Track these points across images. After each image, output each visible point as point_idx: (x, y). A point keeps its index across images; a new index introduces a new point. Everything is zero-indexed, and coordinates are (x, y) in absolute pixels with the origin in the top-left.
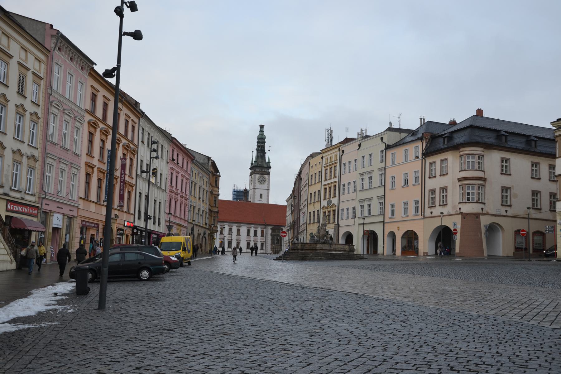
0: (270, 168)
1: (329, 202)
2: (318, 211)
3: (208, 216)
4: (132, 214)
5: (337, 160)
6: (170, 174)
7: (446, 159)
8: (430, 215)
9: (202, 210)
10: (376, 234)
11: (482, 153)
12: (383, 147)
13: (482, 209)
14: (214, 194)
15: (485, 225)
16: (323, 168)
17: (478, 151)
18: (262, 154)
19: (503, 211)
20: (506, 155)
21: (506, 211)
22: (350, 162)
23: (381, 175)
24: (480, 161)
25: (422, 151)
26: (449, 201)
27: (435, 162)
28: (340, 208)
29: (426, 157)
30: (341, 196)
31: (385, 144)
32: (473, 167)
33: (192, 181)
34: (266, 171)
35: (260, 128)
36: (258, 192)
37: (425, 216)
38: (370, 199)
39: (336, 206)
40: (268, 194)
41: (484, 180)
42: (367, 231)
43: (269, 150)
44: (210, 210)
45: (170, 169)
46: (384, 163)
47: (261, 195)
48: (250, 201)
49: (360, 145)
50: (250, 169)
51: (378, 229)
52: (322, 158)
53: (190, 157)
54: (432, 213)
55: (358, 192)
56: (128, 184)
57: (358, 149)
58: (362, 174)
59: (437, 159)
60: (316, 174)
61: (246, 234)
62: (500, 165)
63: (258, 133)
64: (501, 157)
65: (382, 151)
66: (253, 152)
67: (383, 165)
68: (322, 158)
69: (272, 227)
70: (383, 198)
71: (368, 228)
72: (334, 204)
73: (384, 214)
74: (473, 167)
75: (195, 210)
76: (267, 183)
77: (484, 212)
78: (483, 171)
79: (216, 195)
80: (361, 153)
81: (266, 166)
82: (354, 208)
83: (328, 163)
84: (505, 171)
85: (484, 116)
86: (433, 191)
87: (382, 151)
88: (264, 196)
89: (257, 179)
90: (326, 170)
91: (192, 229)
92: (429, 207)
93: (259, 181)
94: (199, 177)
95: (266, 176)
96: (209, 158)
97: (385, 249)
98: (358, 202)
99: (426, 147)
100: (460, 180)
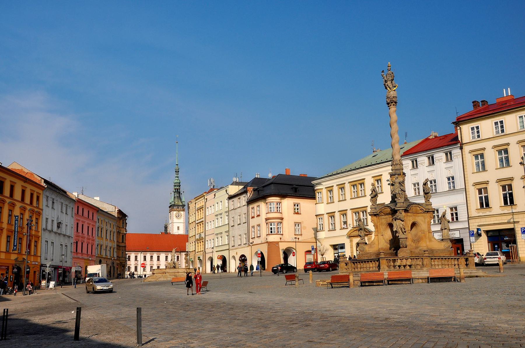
3: (115, 250)
4: (39, 256)
9: (110, 246)
11: (280, 201)
12: (227, 196)
13: (281, 238)
14: (122, 233)
18: (178, 195)
25: (247, 199)
32: (274, 210)
38: (221, 233)
41: (282, 219)
43: (183, 192)
44: (117, 245)
47: (178, 227)
49: (215, 195)
53: (95, 210)
56: (34, 236)
59: (255, 205)
64: (294, 203)
68: (195, 204)
72: (202, 237)
74: (274, 210)
77: (282, 240)
89: (174, 215)
100: (266, 219)
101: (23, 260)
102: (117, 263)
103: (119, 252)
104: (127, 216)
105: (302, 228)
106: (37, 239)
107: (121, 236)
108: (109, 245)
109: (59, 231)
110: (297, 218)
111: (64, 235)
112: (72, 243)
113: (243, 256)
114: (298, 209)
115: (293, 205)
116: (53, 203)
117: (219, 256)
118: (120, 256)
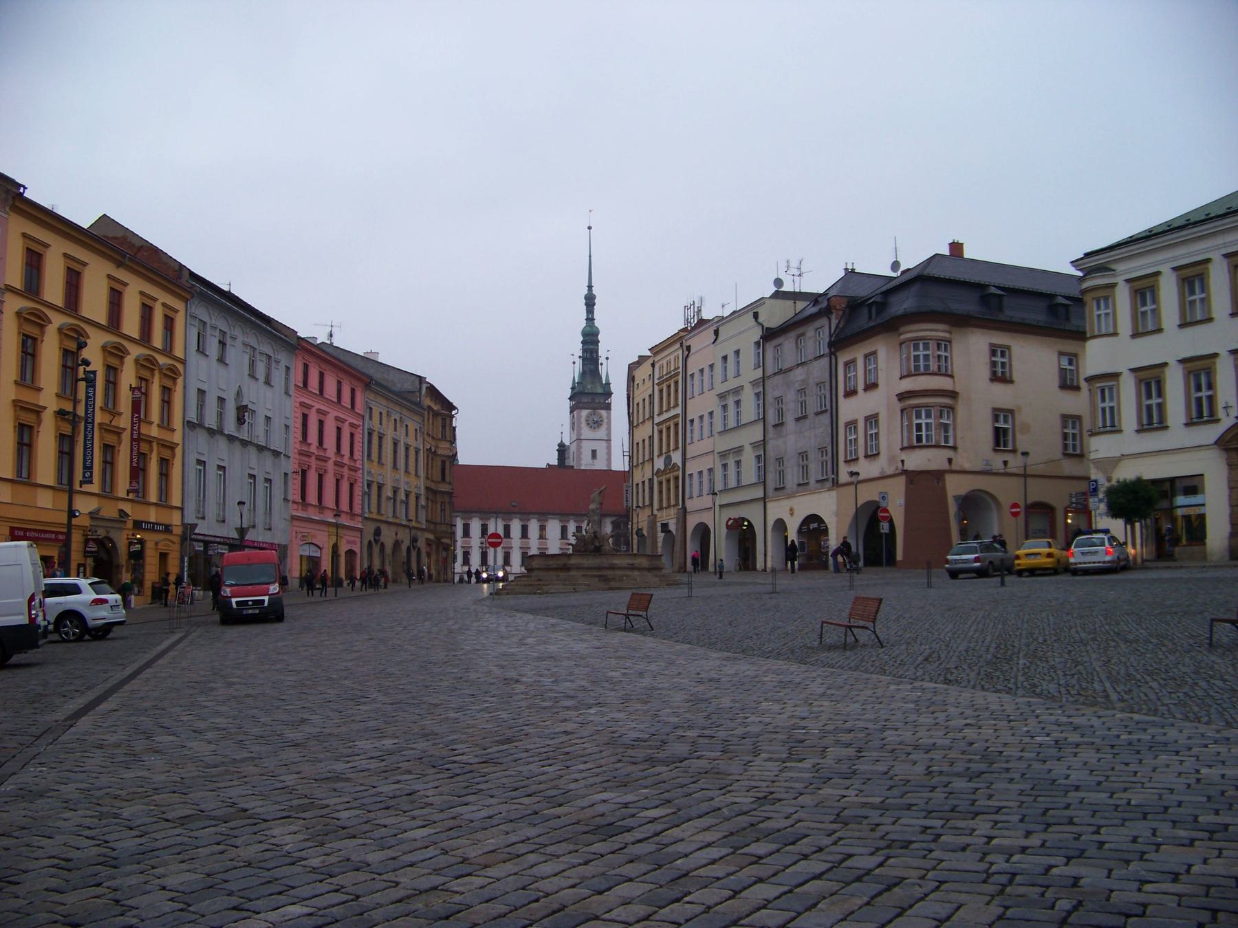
0: (609, 394)
1: (668, 459)
2: (650, 479)
3: (423, 502)
4: (176, 508)
5: (678, 368)
6: (300, 416)
7: (874, 353)
12: (757, 334)
13: (950, 461)
15: (954, 497)
16: (655, 386)
17: (937, 331)
18: (592, 367)
19: (997, 462)
20: (1000, 339)
21: (1005, 463)
22: (702, 371)
24: (942, 353)
25: (831, 336)
27: (854, 361)
28: (688, 472)
29: (837, 350)
30: (688, 448)
31: (763, 326)
33: (369, 429)
34: (602, 401)
35: (587, 312)
36: (587, 448)
38: (739, 450)
39: (679, 467)
40: (609, 448)
41: (953, 395)
43: (607, 358)
44: (427, 488)
45: (298, 405)
47: (594, 453)
48: (572, 467)
49: (716, 333)
50: (571, 399)
51: (753, 515)
52: (653, 365)
53: (359, 379)
55: (716, 436)
56: (158, 444)
57: (714, 343)
58: (722, 396)
59: (858, 353)
60: (644, 400)
61: (559, 535)
62: (988, 361)
63: (584, 324)
64: (991, 345)
65: (757, 343)
66: (574, 363)
67: (759, 373)
68: (653, 365)
69: (614, 519)
71: (735, 513)
75: (384, 490)
76: (604, 426)
77: (954, 467)
78: (951, 376)
79: (443, 456)
80: (720, 350)
81: (600, 391)
82: (710, 470)
83: (663, 377)
84: (1000, 376)
85: (965, 256)
86: (851, 425)
87: (757, 343)
88: (601, 454)
89: (583, 420)
90: (661, 391)
91: (378, 532)
93: (588, 424)
94: (393, 418)
95: (603, 413)
96: (421, 379)
97: (769, 559)
98: (716, 456)
99: (837, 327)
100: (902, 397)
101: (121, 516)
102: (427, 539)
103: (432, 509)
104: (455, 408)
105: (1017, 429)
106: (169, 452)
107: (439, 463)
108: (402, 487)
109: (244, 436)
110: (1002, 395)
111: (261, 449)
112: (286, 474)
113: (813, 518)
114: (1003, 364)
115: (985, 350)
116: (222, 343)
117: (730, 519)
118: (434, 521)
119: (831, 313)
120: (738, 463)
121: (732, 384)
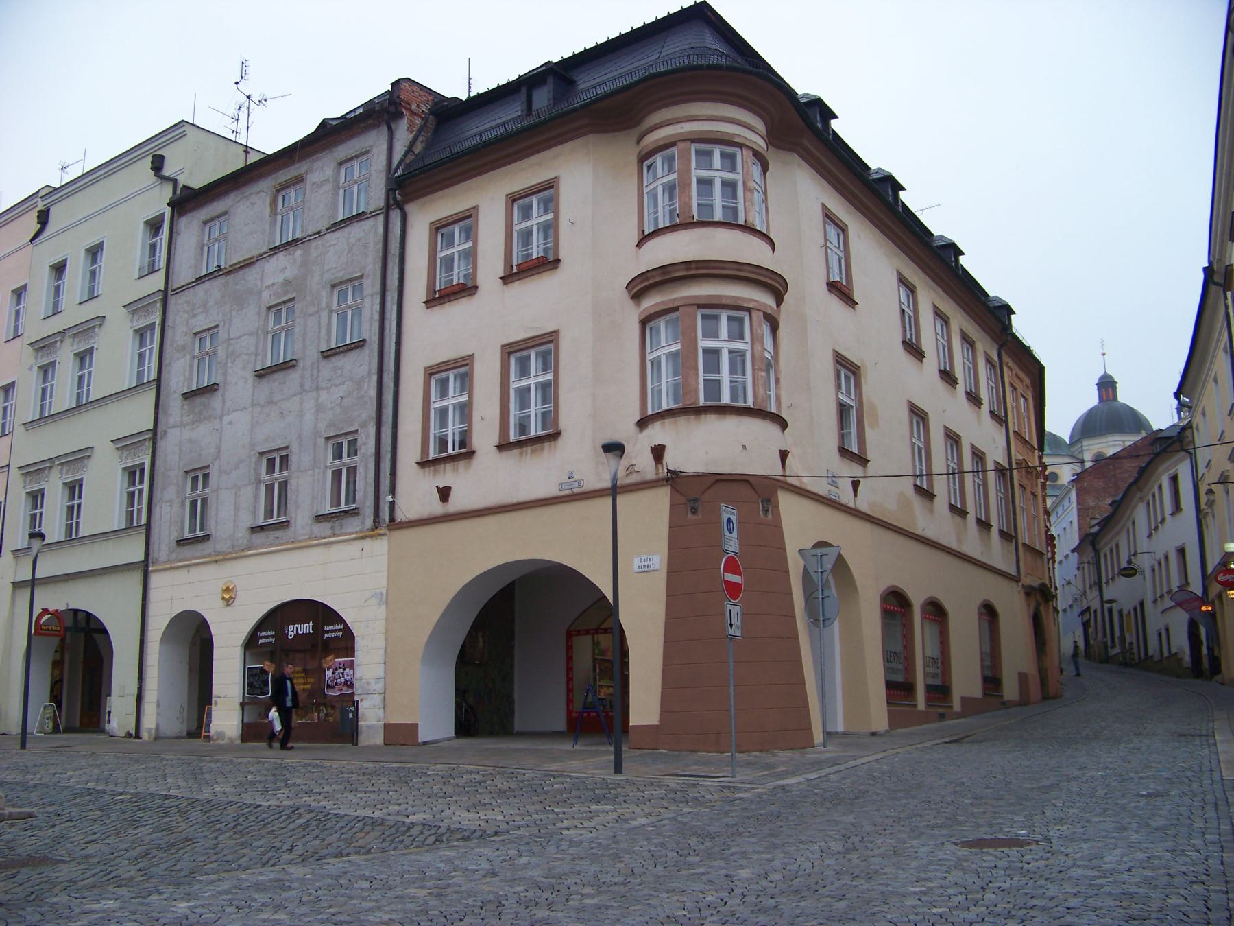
7: (549, 187)
8: (437, 508)
10: (104, 631)
12: (159, 201)
23: (141, 334)
26: (572, 415)
27: (468, 218)
37: (400, 517)
38: (80, 457)
42: (56, 614)
46: (163, 273)
54: (444, 493)
55: (19, 431)
58: (43, 346)
65: (154, 226)
67: (156, 282)
70: (149, 444)
73: (148, 526)
80: (48, 252)
87: (154, 226)
92: (423, 464)
97: (150, 709)
98: (15, 473)
99: (410, 149)
100: (640, 287)
113: (320, 613)
117: (45, 611)
119: (401, 115)
120: (74, 489)
121: (72, 314)
